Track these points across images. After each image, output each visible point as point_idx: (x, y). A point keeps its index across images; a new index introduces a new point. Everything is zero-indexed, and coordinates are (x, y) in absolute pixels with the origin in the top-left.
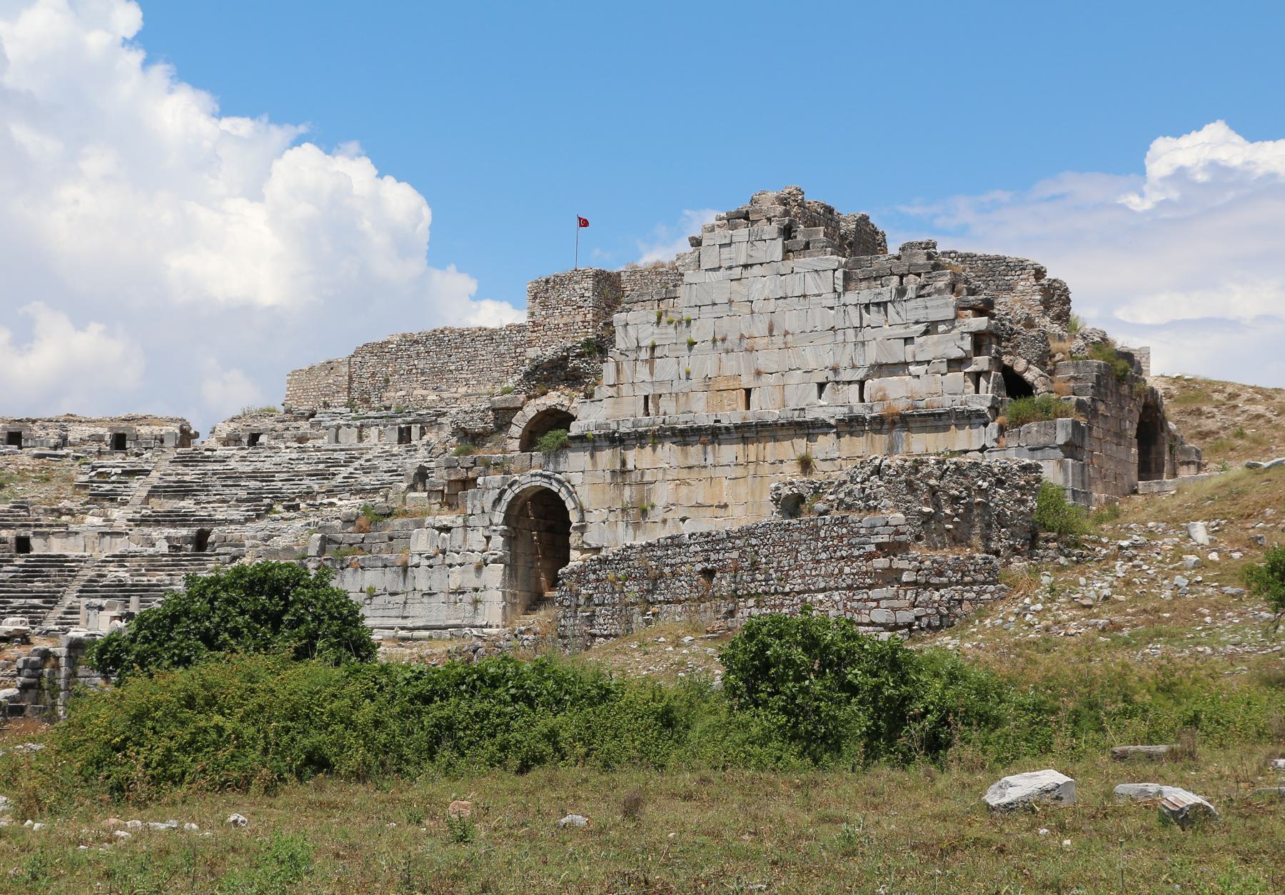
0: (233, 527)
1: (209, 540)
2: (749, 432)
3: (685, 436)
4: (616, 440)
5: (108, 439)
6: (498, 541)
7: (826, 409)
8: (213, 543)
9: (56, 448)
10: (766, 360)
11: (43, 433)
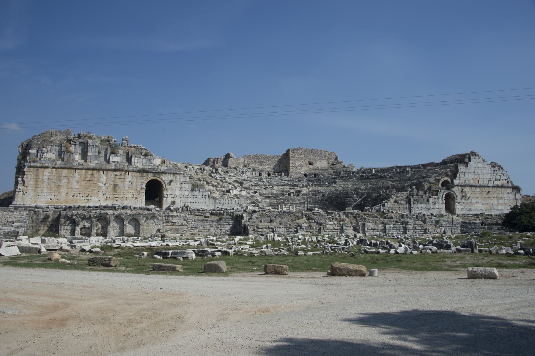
2: (480, 186)
3: (471, 186)
4: (462, 186)
6: (444, 201)
7: (491, 184)
10: (481, 176)
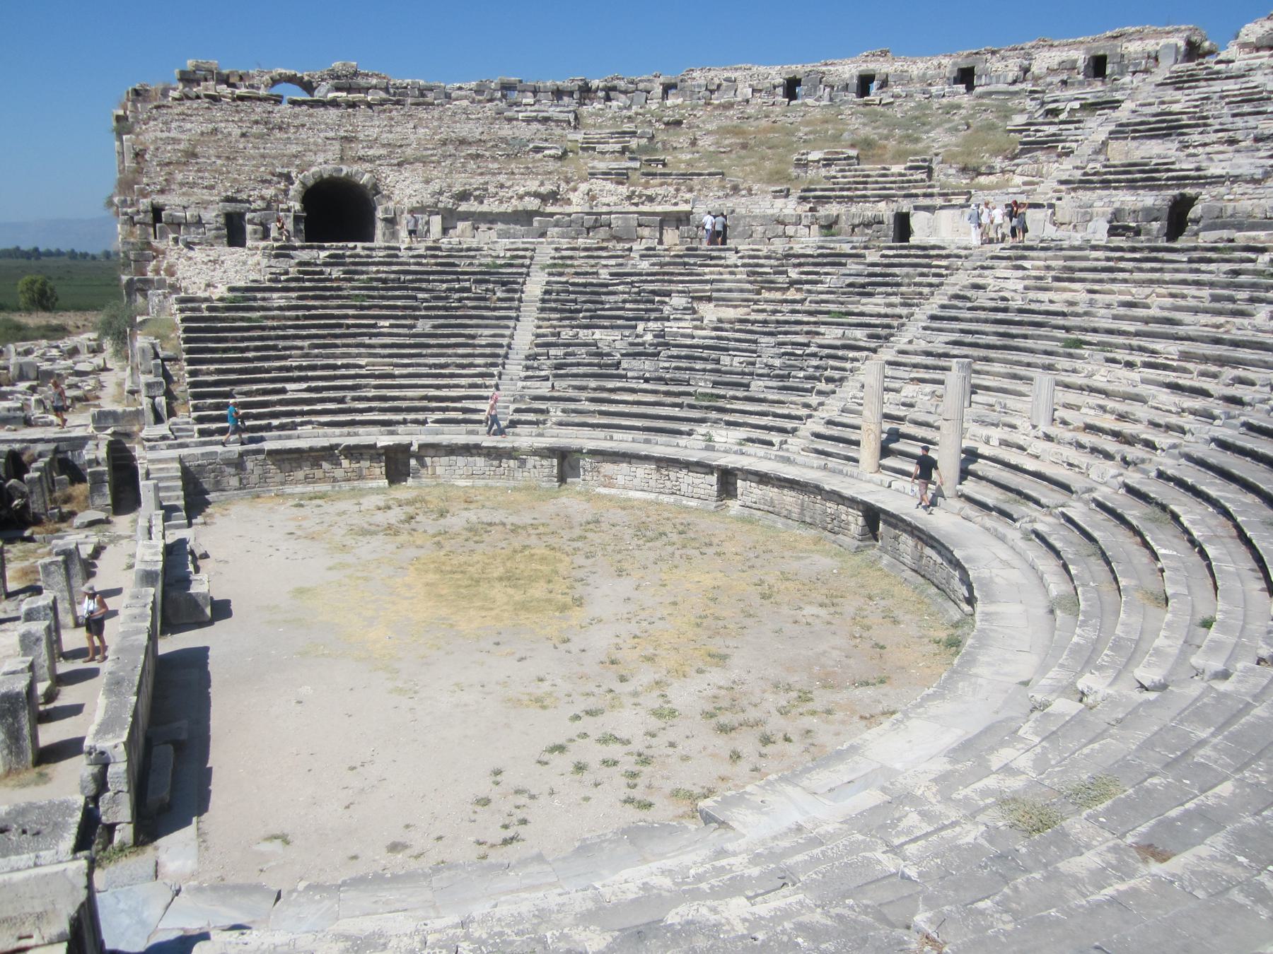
0: (1237, 189)
1: (1191, 215)
5: (1081, 64)
8: (1196, 221)
9: (1014, 82)
11: (1000, 65)
